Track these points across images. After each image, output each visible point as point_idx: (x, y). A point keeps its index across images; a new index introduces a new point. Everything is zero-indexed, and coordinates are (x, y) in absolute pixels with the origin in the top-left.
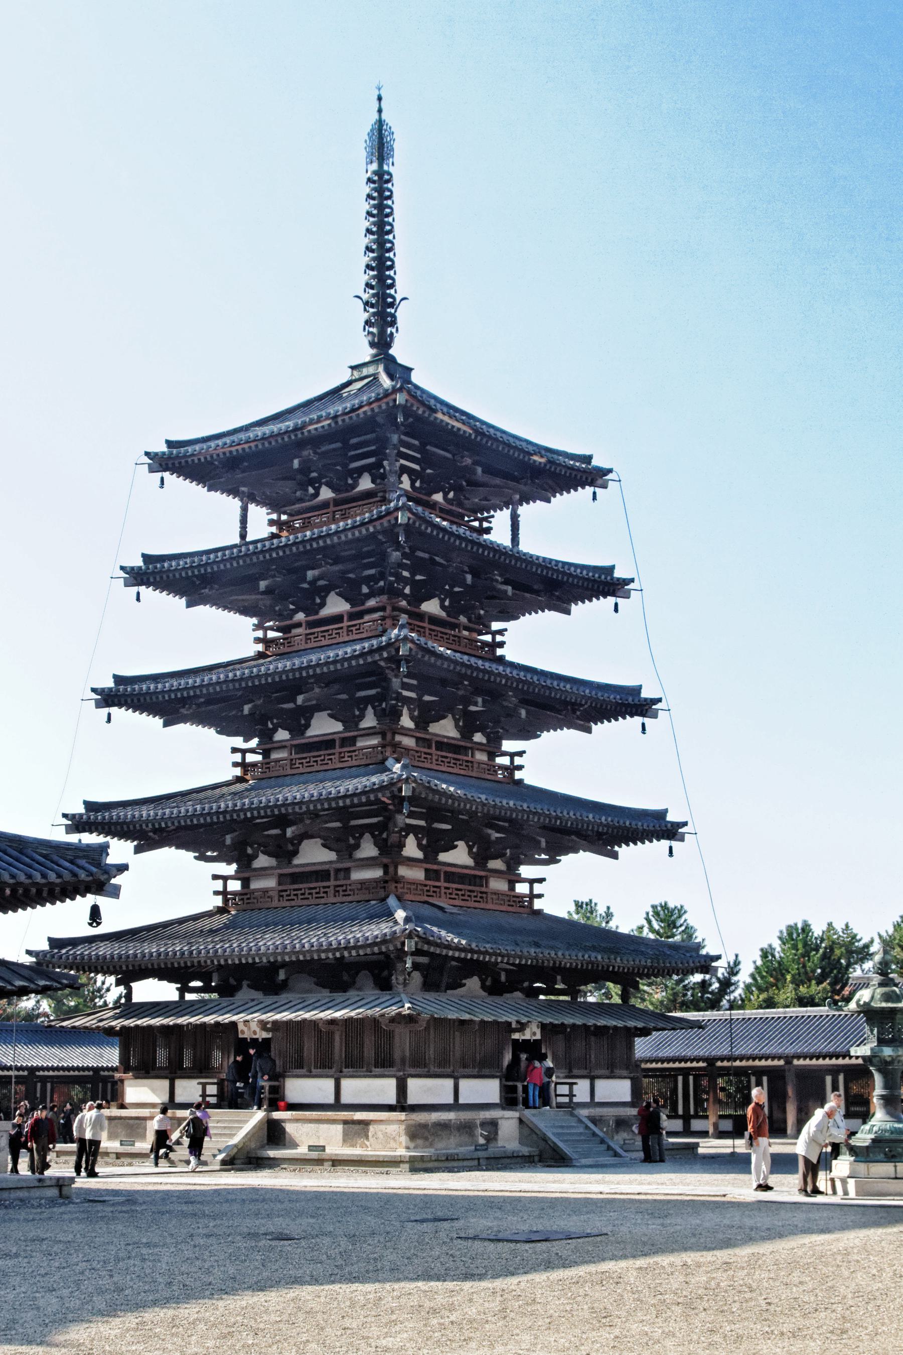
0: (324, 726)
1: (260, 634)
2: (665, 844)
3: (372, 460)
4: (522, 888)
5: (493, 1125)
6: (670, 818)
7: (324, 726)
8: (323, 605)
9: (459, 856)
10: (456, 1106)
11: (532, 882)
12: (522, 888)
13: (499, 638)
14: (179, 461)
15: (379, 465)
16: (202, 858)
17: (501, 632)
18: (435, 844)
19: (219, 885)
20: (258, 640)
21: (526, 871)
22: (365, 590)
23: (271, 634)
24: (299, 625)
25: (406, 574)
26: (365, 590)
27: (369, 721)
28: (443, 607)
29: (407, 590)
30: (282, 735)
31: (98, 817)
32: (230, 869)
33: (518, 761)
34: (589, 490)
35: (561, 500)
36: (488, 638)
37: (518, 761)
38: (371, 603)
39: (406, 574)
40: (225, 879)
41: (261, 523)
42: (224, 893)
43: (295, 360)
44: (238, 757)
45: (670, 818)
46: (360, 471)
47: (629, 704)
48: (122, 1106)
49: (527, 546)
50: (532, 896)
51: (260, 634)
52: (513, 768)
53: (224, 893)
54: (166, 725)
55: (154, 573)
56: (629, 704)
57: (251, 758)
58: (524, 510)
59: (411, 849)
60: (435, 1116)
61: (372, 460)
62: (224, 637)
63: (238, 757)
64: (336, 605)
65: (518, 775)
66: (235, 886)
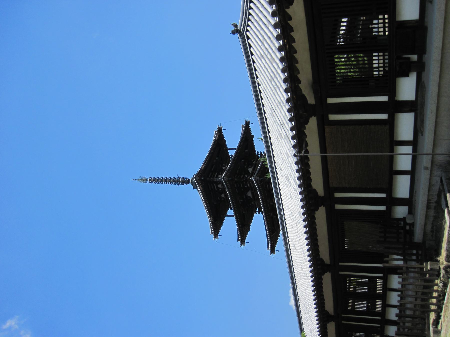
1: (257, 213)
3: (215, 185)
8: (250, 197)
13: (259, 153)
15: (215, 182)
17: (258, 153)
20: (259, 213)
22: (246, 187)
23: (257, 210)
24: (255, 203)
25: (242, 177)
26: (246, 187)
28: (251, 167)
29: (246, 176)
34: (223, 131)
38: (248, 185)
39: (242, 177)
41: (231, 212)
46: (218, 188)
51: (257, 213)
58: (228, 147)
61: (215, 185)
64: (250, 194)
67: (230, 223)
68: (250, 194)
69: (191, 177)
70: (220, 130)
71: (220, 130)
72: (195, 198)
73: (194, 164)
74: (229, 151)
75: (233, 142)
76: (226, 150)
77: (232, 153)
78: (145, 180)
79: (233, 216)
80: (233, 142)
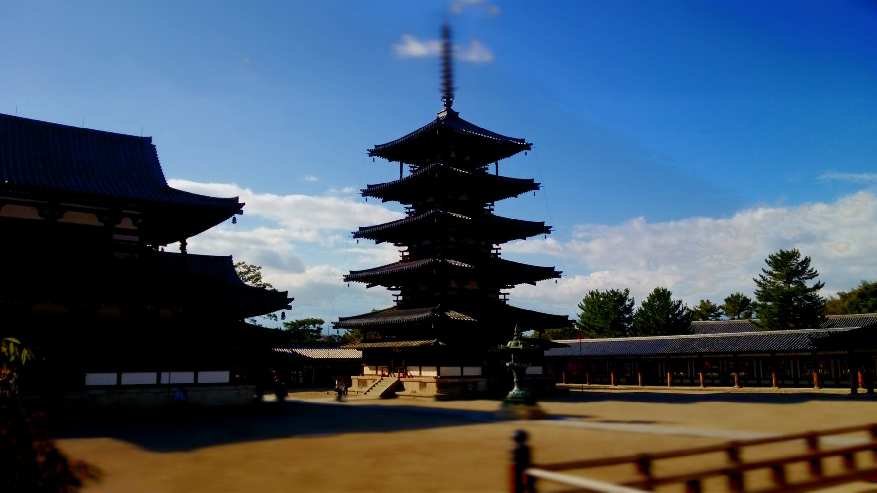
2: (555, 279)
4: (501, 297)
5: (475, 384)
6: (556, 270)
10: (462, 376)
11: (505, 294)
12: (501, 297)
16: (390, 289)
19: (395, 298)
21: (502, 291)
32: (399, 292)
33: (499, 251)
35: (512, 157)
36: (487, 208)
37: (499, 251)
40: (397, 296)
42: (397, 301)
44: (401, 254)
45: (556, 270)
48: (363, 375)
49: (501, 174)
50: (505, 299)
52: (498, 253)
53: (397, 301)
54: (377, 243)
57: (405, 254)
60: (453, 380)
63: (401, 254)
65: (499, 256)
66: (400, 298)
69: (455, 107)
71: (527, 147)
74: (494, 163)
75: (509, 167)
79: (401, 176)
80: (509, 167)
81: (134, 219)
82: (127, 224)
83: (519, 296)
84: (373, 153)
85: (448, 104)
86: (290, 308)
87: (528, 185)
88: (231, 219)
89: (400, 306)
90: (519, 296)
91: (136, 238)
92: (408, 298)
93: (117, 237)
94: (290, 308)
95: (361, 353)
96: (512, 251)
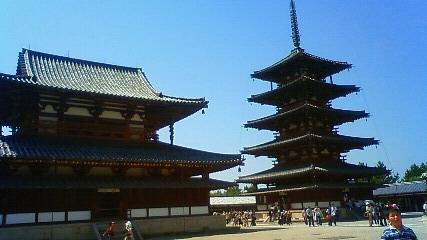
0: (293, 127)
7: (293, 127)
9: (326, 152)
14: (257, 75)
18: (319, 150)
27: (302, 125)
30: (284, 130)
31: (247, 151)
35: (341, 72)
43: (280, 52)
47: (362, 115)
55: (254, 99)
56: (362, 115)
58: (333, 76)
59: (314, 152)
62: (270, 110)
64: (292, 101)
67: (265, 87)
68: (292, 101)
70: (348, 66)
72: (281, 52)
73: (315, 48)
75: (338, 79)
76: (330, 74)
77: (328, 80)
78: (293, 5)
80: (338, 79)
81: (140, 114)
82: (136, 118)
83: (352, 157)
84: (253, 76)
85: (297, 44)
86: (243, 165)
87: (353, 89)
88: (201, 111)
89: (276, 169)
90: (352, 157)
91: (142, 126)
92: (283, 162)
93: (132, 126)
94: (243, 165)
95: (254, 198)
96: (345, 130)
